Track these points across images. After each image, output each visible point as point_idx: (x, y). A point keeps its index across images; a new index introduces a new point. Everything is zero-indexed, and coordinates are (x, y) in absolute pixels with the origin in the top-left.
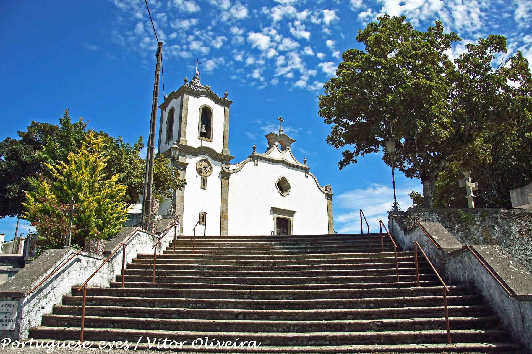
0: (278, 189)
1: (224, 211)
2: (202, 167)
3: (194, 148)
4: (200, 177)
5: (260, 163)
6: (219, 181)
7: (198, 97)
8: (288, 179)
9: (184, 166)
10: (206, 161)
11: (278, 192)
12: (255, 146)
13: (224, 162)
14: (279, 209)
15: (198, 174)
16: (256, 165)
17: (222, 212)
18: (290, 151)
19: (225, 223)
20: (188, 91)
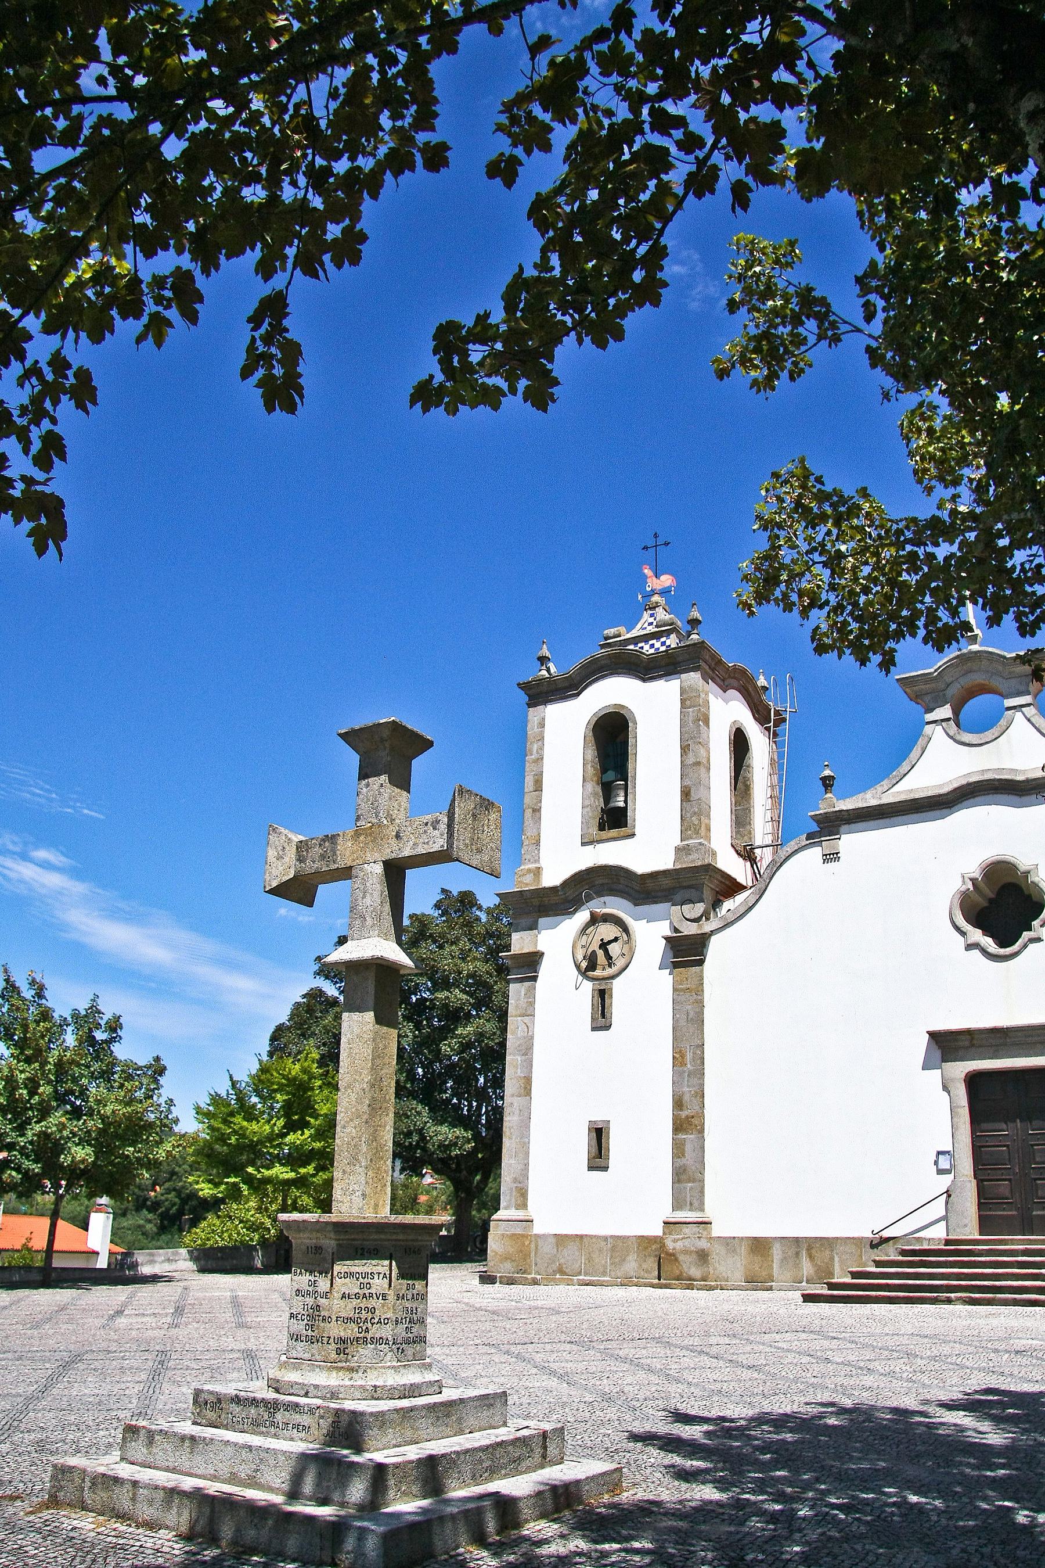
0: (963, 933)
1: (686, 1098)
2: (595, 946)
3: (554, 889)
4: (588, 986)
5: (849, 842)
6: (666, 979)
7: (578, 694)
8: (1024, 863)
9: (531, 962)
10: (595, 920)
11: (969, 947)
12: (827, 772)
13: (678, 897)
14: (969, 1032)
15: (580, 978)
16: (831, 857)
17: (678, 1103)
18: (1030, 711)
19: (688, 1148)
20: (541, 693)
